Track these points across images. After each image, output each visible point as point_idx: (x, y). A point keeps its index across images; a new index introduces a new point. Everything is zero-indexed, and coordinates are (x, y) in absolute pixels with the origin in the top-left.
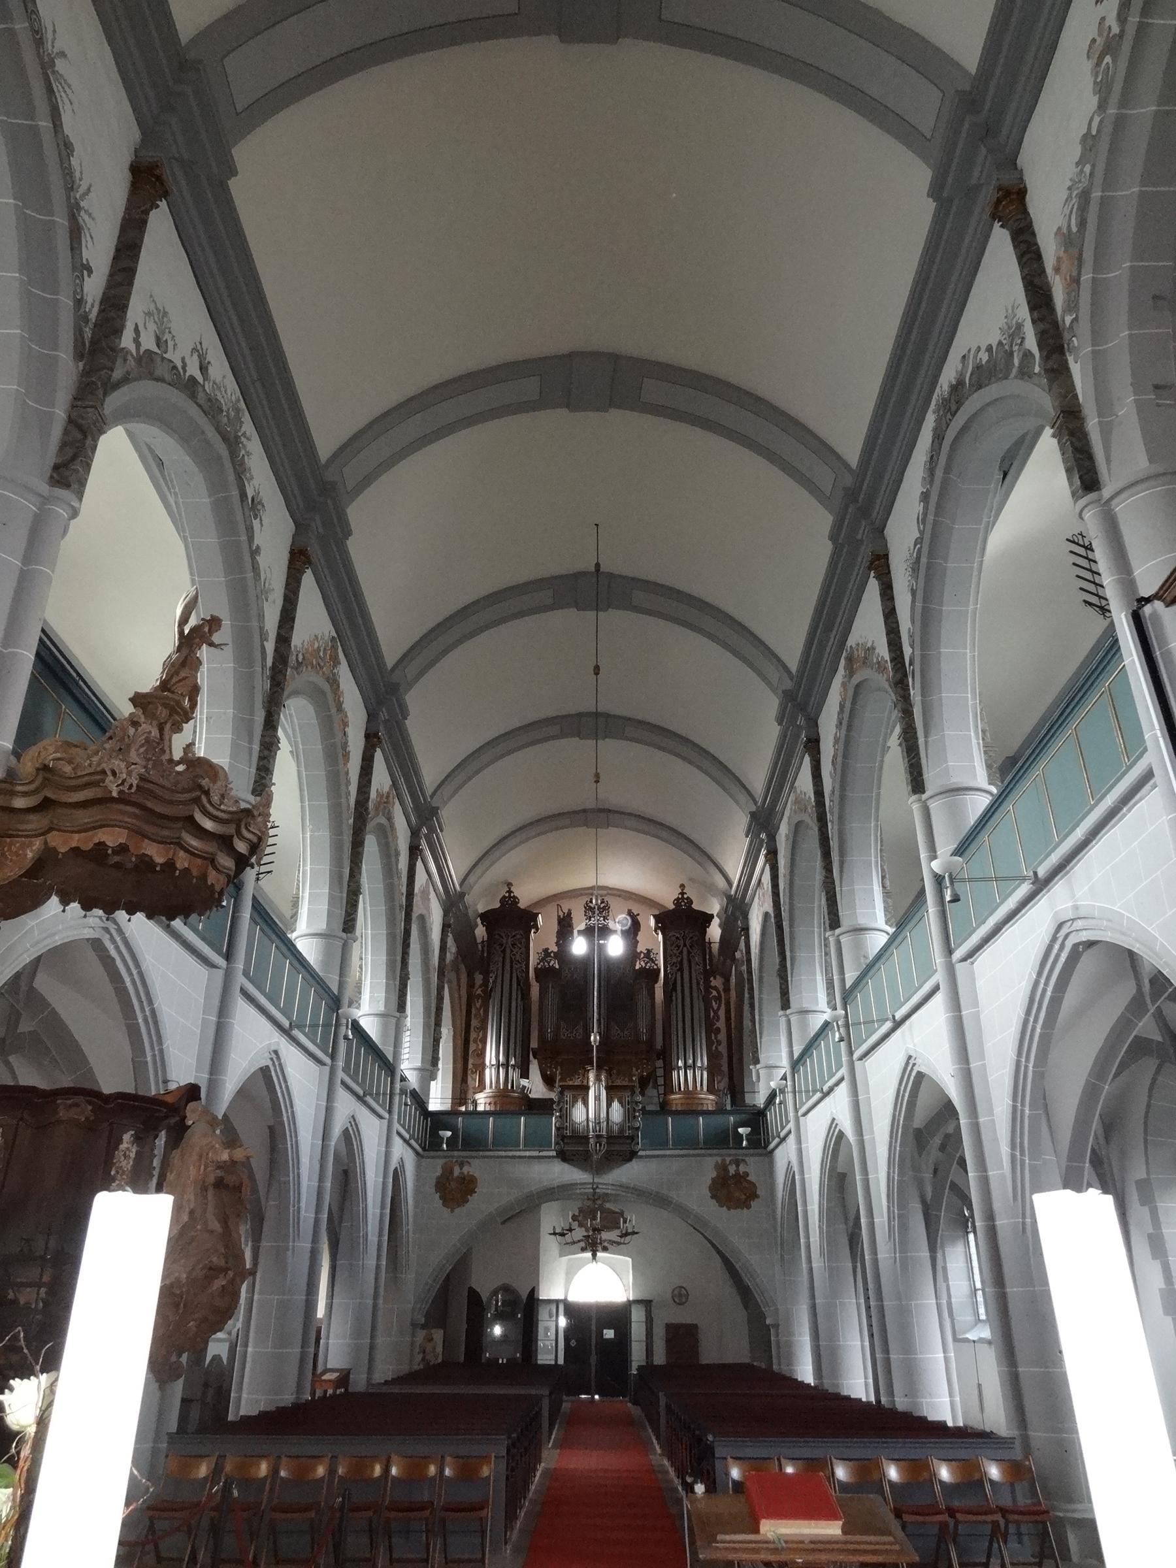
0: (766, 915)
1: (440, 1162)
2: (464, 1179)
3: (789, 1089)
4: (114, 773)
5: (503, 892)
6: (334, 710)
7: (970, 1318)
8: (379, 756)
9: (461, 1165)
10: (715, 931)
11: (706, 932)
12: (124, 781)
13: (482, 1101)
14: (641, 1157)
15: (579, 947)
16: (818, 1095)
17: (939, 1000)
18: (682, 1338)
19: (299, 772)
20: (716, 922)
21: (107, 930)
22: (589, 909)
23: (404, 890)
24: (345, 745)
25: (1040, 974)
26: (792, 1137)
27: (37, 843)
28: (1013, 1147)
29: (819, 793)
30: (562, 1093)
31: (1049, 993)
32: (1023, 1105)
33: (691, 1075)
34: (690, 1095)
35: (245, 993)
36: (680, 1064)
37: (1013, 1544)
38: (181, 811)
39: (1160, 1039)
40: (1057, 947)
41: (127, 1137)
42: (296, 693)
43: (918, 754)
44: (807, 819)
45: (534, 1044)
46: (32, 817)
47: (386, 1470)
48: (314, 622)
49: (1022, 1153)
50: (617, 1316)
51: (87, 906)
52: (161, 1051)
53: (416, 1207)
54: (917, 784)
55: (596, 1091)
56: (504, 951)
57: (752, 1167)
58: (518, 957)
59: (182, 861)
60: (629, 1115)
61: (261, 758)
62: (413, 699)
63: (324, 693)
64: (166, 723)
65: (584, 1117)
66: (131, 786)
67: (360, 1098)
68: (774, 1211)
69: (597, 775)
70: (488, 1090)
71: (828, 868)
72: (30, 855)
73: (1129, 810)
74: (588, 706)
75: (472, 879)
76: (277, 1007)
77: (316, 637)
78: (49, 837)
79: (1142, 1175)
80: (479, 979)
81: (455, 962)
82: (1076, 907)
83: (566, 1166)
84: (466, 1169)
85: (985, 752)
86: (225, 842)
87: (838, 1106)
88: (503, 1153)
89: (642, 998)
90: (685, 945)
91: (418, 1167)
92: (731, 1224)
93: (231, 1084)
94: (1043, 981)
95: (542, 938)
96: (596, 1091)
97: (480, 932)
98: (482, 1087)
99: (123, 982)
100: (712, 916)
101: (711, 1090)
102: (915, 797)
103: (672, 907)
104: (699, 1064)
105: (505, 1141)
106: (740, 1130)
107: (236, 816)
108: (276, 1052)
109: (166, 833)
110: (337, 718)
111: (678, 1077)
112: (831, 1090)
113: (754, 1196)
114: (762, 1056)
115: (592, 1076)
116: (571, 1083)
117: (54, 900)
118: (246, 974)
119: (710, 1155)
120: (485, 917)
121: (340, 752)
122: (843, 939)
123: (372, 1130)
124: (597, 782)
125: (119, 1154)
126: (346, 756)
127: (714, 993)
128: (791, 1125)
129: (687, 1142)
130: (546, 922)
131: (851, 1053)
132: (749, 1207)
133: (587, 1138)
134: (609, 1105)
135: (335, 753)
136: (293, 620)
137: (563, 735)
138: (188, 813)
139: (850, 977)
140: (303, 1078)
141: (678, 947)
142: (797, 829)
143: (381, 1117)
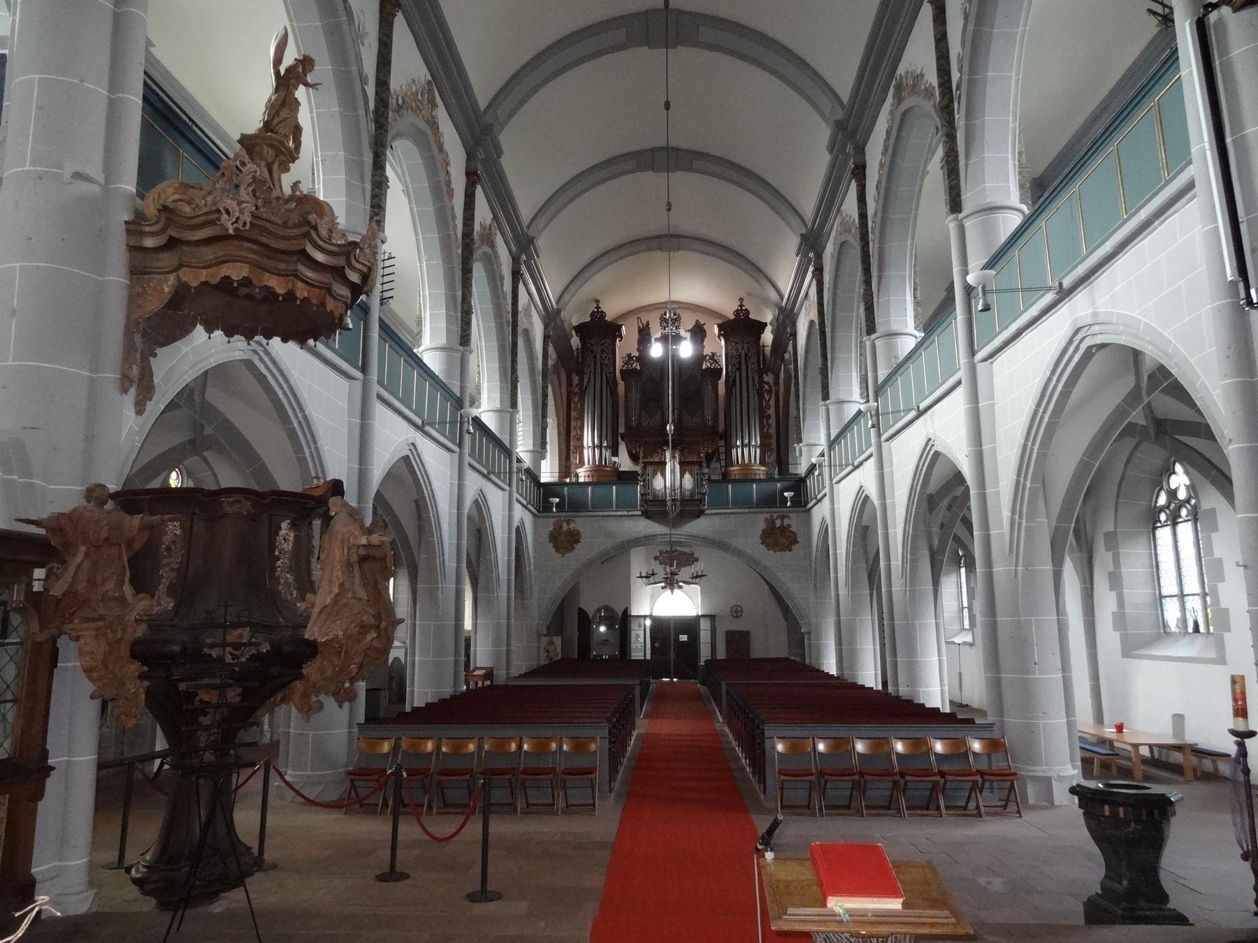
0: (812, 323)
1: (551, 521)
3: (826, 463)
4: (228, 212)
5: (593, 308)
6: (436, 151)
7: (957, 627)
8: (479, 191)
9: (568, 522)
10: (768, 337)
11: (759, 338)
12: (238, 218)
13: (583, 474)
15: (656, 351)
16: (850, 468)
17: (960, 392)
18: (738, 640)
19: (411, 209)
20: (769, 329)
21: (255, 352)
22: (663, 320)
23: (510, 309)
24: (449, 183)
25: (1053, 372)
26: (827, 499)
27: (172, 279)
28: (1013, 513)
29: (863, 216)
30: (644, 468)
31: (1059, 389)
32: (1025, 479)
33: (747, 451)
34: (746, 467)
35: (379, 397)
37: (986, 793)
38: (294, 246)
39: (1144, 422)
40: (1072, 349)
41: (284, 525)
42: (399, 135)
43: (958, 177)
44: (852, 241)
45: (622, 430)
46: (163, 255)
47: (520, 747)
48: (409, 67)
49: (1020, 518)
50: (689, 626)
51: (229, 333)
52: (317, 448)
53: (535, 550)
54: (955, 204)
55: (672, 466)
56: (595, 357)
57: (794, 521)
59: (302, 291)
60: (698, 483)
61: (373, 197)
62: (506, 139)
63: (424, 134)
64: (273, 163)
66: (245, 224)
67: (486, 477)
68: (810, 553)
69: (669, 204)
70: (586, 465)
71: (867, 281)
72: (167, 290)
73: (1160, 224)
74: (661, 143)
75: (566, 297)
76: (410, 408)
77: (413, 81)
78: (181, 272)
79: (1109, 527)
80: (576, 379)
81: (554, 366)
82: (1095, 314)
83: (649, 522)
84: (572, 525)
85: (1020, 173)
86: (339, 273)
87: (866, 477)
89: (708, 394)
91: (535, 528)
92: (774, 560)
93: (378, 472)
94: (1055, 378)
95: (626, 346)
96: (672, 466)
97: (575, 341)
98: (582, 463)
99: (276, 394)
100: (765, 324)
101: (762, 463)
102: (952, 217)
103: (732, 317)
105: (602, 505)
106: (786, 494)
107: (344, 249)
108: (413, 444)
109: (283, 266)
110: (439, 158)
111: (737, 453)
112: (861, 464)
113: (795, 542)
114: (804, 437)
115: (668, 455)
117: (200, 330)
118: (380, 383)
120: (580, 329)
121: (444, 189)
122: (878, 343)
123: (497, 500)
124: (669, 210)
125: (280, 539)
126: (450, 193)
127: (767, 387)
128: (827, 490)
129: (744, 503)
130: (629, 331)
131: (879, 435)
132: (790, 550)
133: (665, 501)
134: (682, 476)
135: (440, 191)
136: (389, 62)
137: (639, 168)
138: (300, 247)
139: (882, 374)
140: (437, 463)
142: (842, 247)
143: (503, 489)
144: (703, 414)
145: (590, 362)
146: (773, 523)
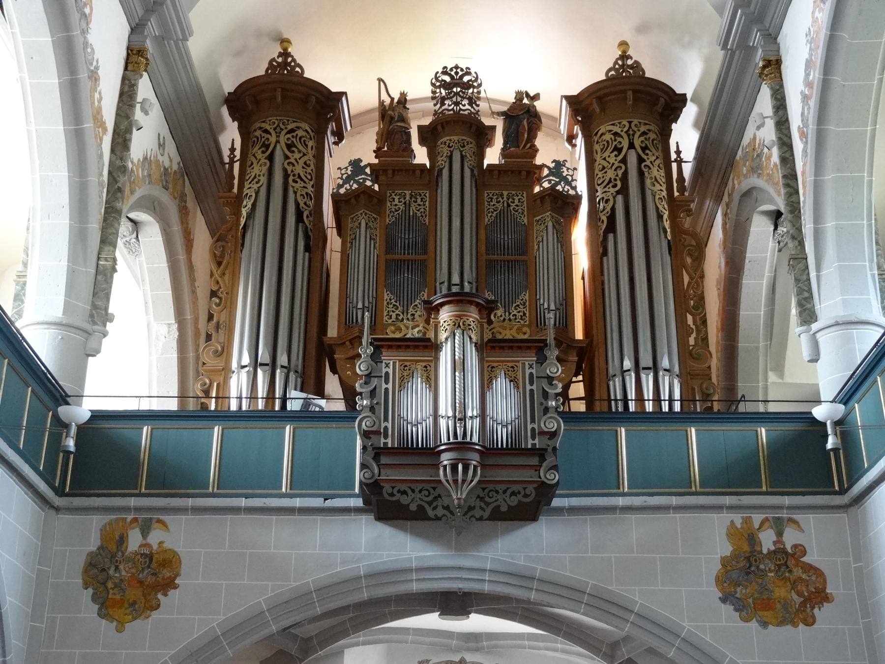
1: (96, 522)
2: (150, 557)
9: (145, 532)
10: (685, 136)
11: (665, 134)
14: (560, 511)
20: (690, 112)
30: (375, 357)
36: (628, 364)
55: (454, 351)
56: (271, 158)
57: (813, 532)
58: (299, 169)
60: (534, 405)
65: (428, 409)
84: (155, 537)
88: (243, 502)
89: (544, 249)
90: (631, 146)
97: (231, 135)
104: (665, 363)
105: (246, 479)
113: (821, 596)
116: (398, 335)
119: (719, 508)
129: (664, 479)
132: (810, 622)
141: (618, 150)
144: (535, 301)
145: (259, 169)
146: (752, 539)
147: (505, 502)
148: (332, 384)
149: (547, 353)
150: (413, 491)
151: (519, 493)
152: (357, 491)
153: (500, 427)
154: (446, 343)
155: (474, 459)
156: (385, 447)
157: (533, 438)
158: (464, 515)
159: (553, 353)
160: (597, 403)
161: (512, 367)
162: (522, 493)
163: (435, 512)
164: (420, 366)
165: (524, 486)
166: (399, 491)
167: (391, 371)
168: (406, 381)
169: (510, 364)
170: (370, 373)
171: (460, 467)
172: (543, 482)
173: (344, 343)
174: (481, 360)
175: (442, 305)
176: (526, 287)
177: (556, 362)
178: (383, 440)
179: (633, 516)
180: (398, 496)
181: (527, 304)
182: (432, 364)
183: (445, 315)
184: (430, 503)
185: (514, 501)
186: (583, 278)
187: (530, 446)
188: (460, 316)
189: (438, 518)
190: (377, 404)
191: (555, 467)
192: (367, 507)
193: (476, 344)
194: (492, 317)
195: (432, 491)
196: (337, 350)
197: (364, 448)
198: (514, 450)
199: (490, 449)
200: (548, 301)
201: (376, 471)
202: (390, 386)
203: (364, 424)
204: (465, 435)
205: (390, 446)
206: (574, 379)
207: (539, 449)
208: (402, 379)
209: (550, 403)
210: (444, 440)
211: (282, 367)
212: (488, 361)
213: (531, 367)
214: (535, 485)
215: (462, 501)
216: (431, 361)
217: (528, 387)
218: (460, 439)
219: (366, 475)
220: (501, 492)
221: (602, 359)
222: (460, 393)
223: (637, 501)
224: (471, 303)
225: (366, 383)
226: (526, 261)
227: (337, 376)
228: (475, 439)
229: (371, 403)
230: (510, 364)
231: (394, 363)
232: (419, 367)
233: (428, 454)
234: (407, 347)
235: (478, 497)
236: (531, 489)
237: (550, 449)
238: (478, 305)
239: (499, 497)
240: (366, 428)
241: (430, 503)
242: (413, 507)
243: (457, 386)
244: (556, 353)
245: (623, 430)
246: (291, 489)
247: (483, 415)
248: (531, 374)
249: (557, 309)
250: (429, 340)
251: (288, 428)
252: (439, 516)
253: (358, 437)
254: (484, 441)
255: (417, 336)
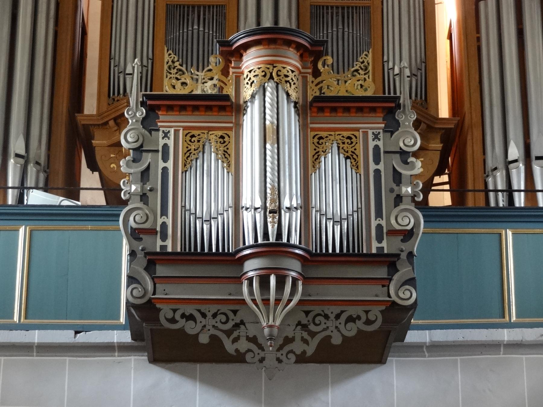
30: (149, 123)
36: (514, 152)
55: (265, 114)
60: (381, 192)
144: (381, 63)
147: (338, 332)
148: (89, 179)
149: (400, 117)
150: (204, 315)
151: (359, 317)
152: (123, 319)
153: (330, 224)
154: (252, 102)
155: (293, 269)
156: (163, 252)
157: (380, 239)
158: (278, 350)
159: (407, 118)
160: (470, 195)
161: (349, 138)
162: (364, 318)
163: (236, 345)
164: (214, 136)
165: (367, 308)
166: (183, 316)
167: (171, 143)
168: (193, 157)
169: (346, 134)
170: (142, 146)
171: (273, 280)
172: (394, 303)
173: (106, 123)
174: (304, 128)
175: (246, 47)
176: (369, 45)
177: (412, 130)
178: (159, 243)
179: (524, 356)
180: (181, 323)
181: (370, 68)
182: (232, 134)
183: (251, 61)
184: (228, 333)
185: (351, 330)
186: (450, 37)
187: (374, 251)
188: (272, 64)
189: (239, 358)
190: (151, 190)
191: (411, 282)
192: (136, 344)
193: (296, 103)
194: (320, 66)
195: (231, 315)
196: (97, 133)
197: (132, 254)
198: (352, 256)
199: (316, 255)
200: (400, 64)
201: (150, 286)
202: (170, 165)
203: (131, 219)
204: (279, 235)
205: (170, 250)
206: (437, 180)
207: (388, 255)
208: (188, 153)
209: (404, 189)
210: (250, 241)
211: (17, 155)
212: (313, 129)
213: (376, 137)
214: (383, 308)
215: (276, 330)
216: (230, 129)
217: (372, 167)
218: (272, 239)
219: (135, 292)
220: (332, 317)
221: (478, 148)
222: (273, 174)
223: (530, 335)
224: (288, 43)
225: (134, 161)
226: (369, 7)
227: (96, 174)
228: (295, 240)
229: (142, 188)
230: (346, 134)
231: (176, 132)
232: (213, 138)
233: (226, 261)
234: (196, 108)
235: (299, 324)
236: (376, 313)
237: (404, 256)
238: (299, 47)
239: (329, 323)
240: (134, 225)
241: (228, 333)
242: (204, 339)
243: (268, 163)
244: (414, 117)
245: (510, 233)
246: (26, 318)
247: (306, 207)
248: (377, 148)
249: (413, 75)
250: (227, 98)
251: (22, 230)
252: (242, 350)
253: (125, 241)
254: (307, 244)
255: (210, 92)
